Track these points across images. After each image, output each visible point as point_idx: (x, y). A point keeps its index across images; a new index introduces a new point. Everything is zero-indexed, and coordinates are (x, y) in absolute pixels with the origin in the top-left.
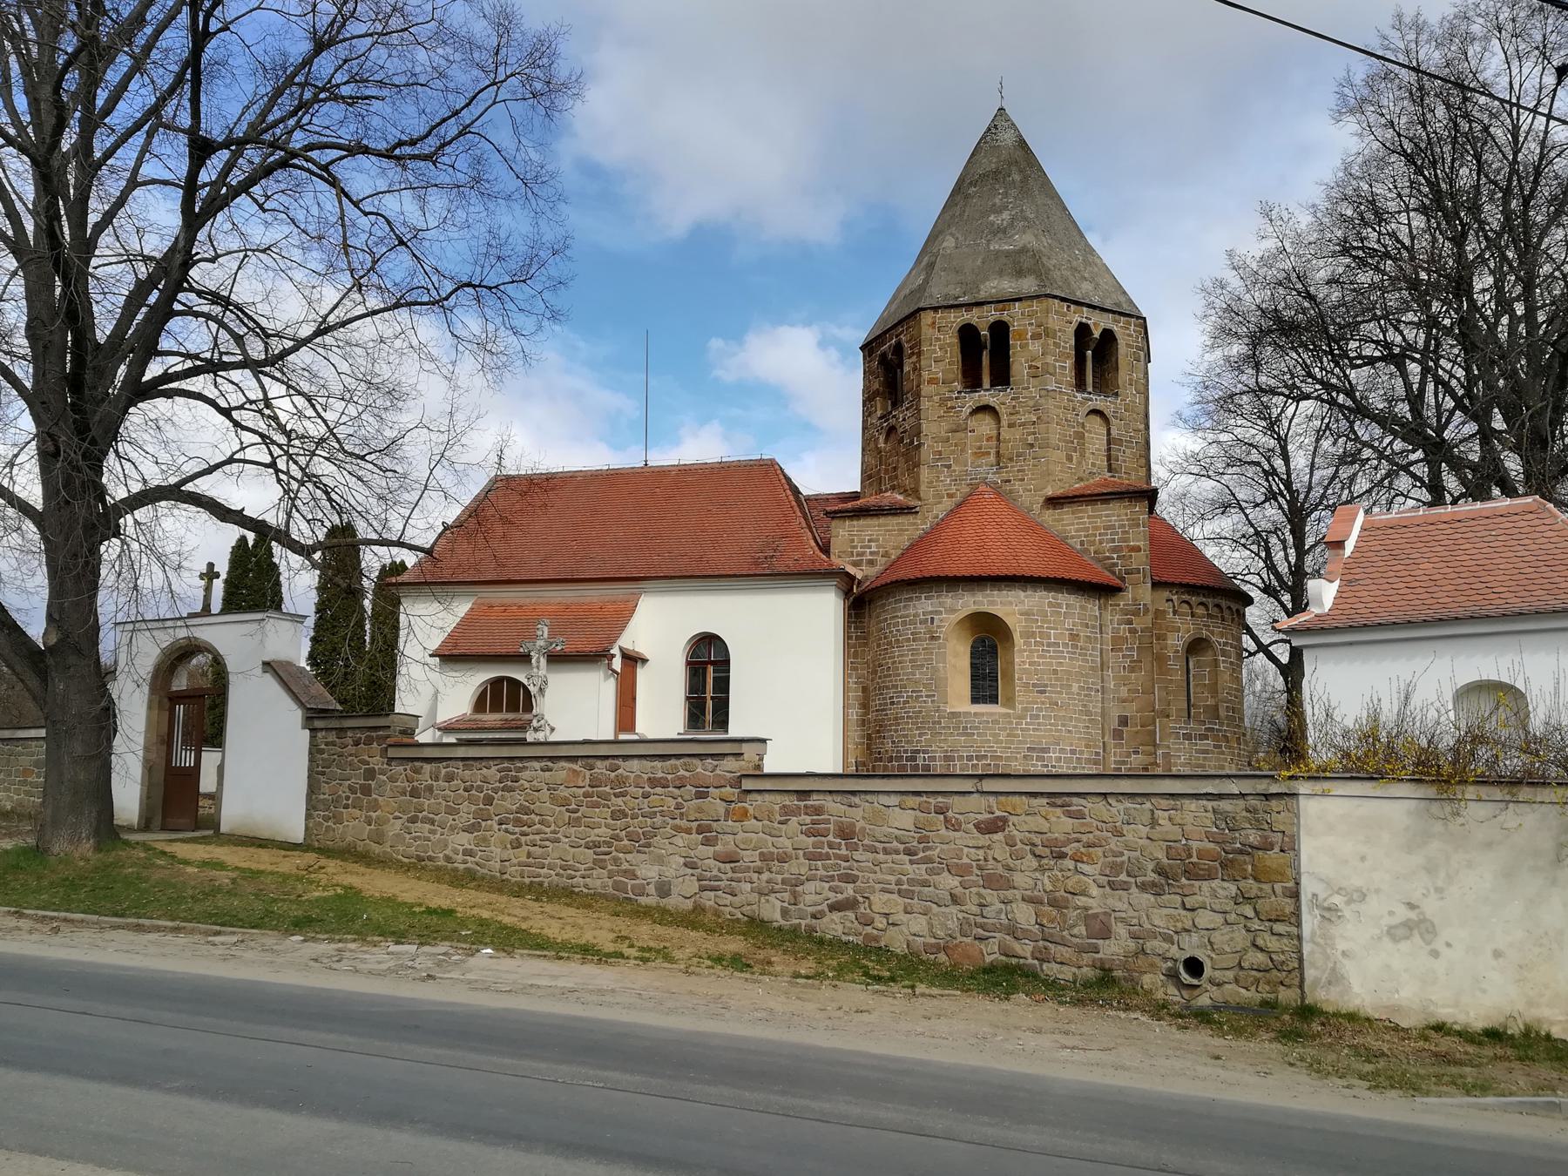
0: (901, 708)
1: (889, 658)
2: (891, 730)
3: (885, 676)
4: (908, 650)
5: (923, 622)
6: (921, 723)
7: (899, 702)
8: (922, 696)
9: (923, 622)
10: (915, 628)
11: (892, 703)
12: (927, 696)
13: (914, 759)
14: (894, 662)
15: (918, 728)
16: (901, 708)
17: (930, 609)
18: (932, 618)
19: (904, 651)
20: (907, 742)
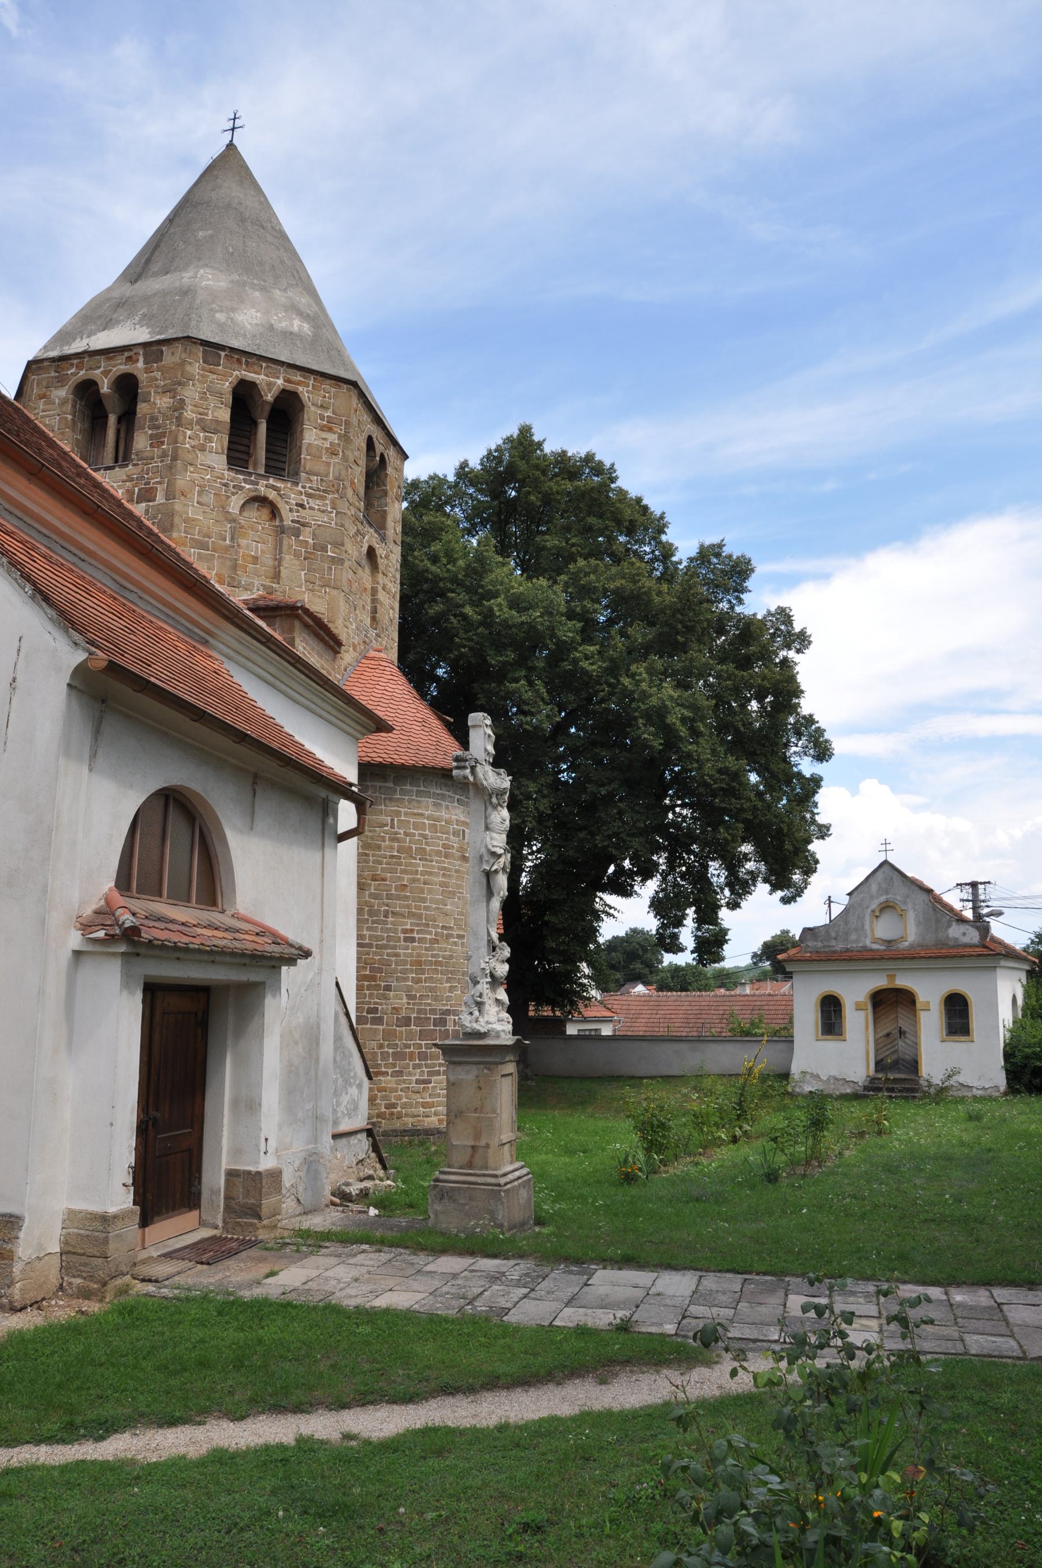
0: (426, 949)
1: (405, 872)
2: (406, 979)
3: (398, 898)
4: (439, 868)
5: (456, 833)
6: (452, 972)
7: (421, 940)
8: (452, 936)
9: (456, 833)
10: (447, 839)
11: (413, 940)
12: (460, 937)
13: (442, 1022)
14: (414, 881)
15: (449, 980)
16: (426, 949)
17: (462, 819)
18: (464, 831)
19: (433, 867)
20: (436, 999)
